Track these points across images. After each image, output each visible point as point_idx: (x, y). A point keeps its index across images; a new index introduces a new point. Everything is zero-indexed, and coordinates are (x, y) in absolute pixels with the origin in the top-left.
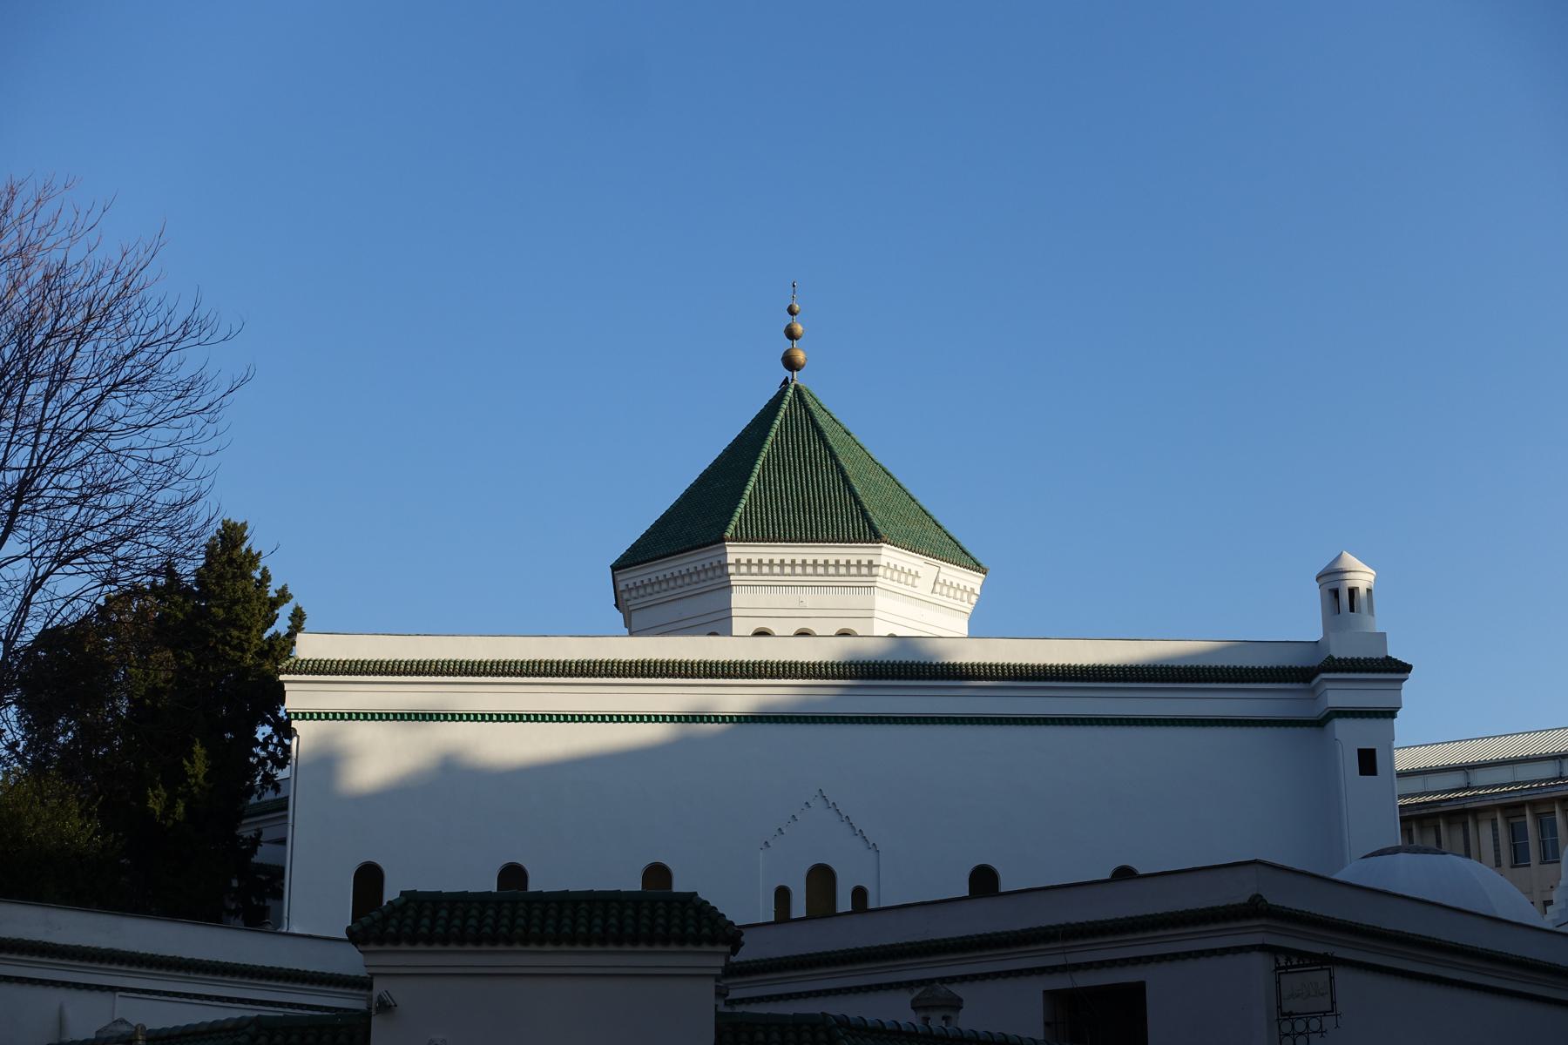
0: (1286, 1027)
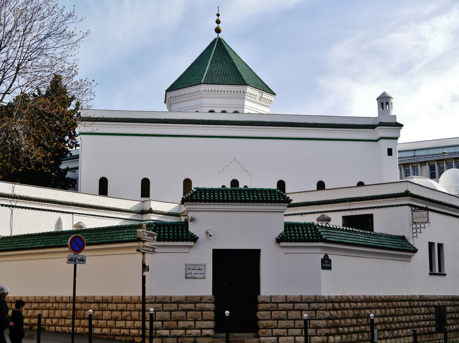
0: (414, 226)
